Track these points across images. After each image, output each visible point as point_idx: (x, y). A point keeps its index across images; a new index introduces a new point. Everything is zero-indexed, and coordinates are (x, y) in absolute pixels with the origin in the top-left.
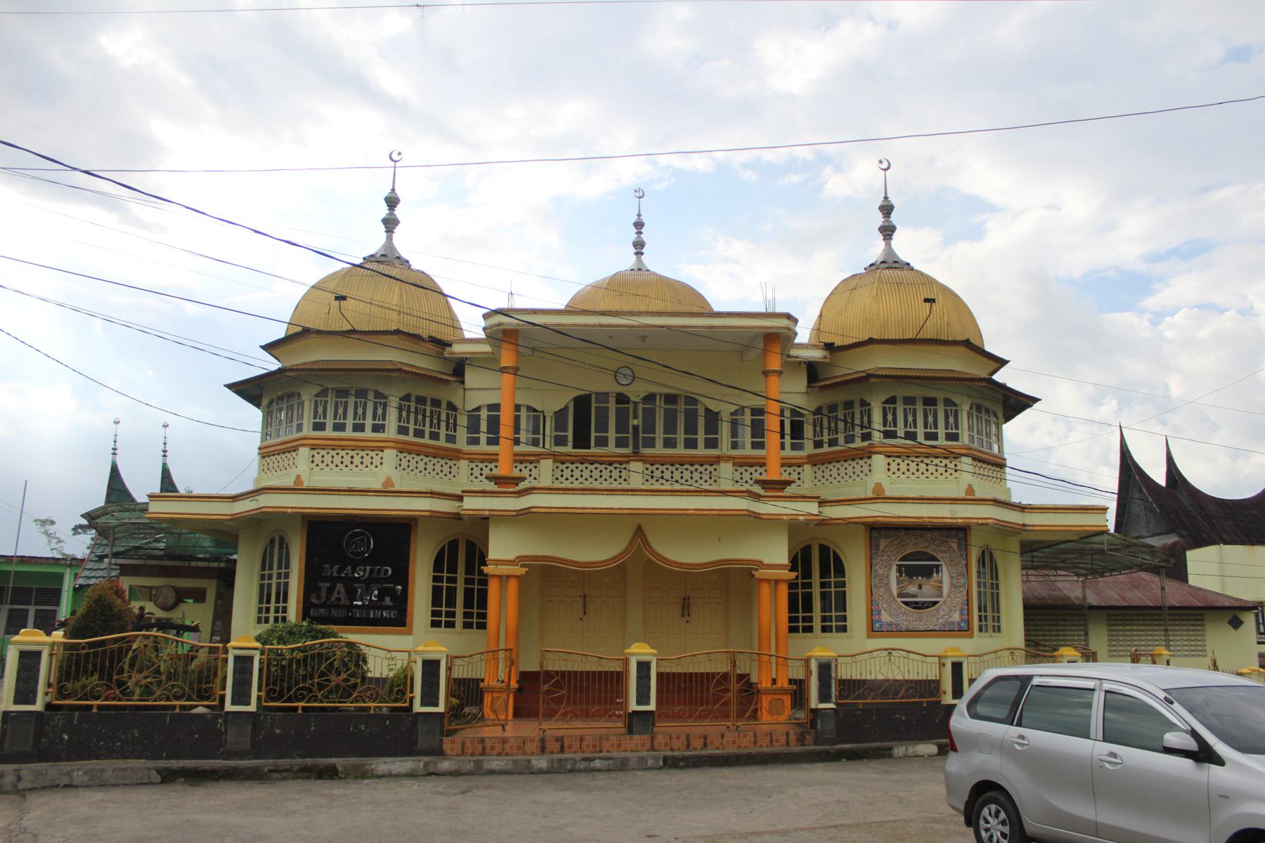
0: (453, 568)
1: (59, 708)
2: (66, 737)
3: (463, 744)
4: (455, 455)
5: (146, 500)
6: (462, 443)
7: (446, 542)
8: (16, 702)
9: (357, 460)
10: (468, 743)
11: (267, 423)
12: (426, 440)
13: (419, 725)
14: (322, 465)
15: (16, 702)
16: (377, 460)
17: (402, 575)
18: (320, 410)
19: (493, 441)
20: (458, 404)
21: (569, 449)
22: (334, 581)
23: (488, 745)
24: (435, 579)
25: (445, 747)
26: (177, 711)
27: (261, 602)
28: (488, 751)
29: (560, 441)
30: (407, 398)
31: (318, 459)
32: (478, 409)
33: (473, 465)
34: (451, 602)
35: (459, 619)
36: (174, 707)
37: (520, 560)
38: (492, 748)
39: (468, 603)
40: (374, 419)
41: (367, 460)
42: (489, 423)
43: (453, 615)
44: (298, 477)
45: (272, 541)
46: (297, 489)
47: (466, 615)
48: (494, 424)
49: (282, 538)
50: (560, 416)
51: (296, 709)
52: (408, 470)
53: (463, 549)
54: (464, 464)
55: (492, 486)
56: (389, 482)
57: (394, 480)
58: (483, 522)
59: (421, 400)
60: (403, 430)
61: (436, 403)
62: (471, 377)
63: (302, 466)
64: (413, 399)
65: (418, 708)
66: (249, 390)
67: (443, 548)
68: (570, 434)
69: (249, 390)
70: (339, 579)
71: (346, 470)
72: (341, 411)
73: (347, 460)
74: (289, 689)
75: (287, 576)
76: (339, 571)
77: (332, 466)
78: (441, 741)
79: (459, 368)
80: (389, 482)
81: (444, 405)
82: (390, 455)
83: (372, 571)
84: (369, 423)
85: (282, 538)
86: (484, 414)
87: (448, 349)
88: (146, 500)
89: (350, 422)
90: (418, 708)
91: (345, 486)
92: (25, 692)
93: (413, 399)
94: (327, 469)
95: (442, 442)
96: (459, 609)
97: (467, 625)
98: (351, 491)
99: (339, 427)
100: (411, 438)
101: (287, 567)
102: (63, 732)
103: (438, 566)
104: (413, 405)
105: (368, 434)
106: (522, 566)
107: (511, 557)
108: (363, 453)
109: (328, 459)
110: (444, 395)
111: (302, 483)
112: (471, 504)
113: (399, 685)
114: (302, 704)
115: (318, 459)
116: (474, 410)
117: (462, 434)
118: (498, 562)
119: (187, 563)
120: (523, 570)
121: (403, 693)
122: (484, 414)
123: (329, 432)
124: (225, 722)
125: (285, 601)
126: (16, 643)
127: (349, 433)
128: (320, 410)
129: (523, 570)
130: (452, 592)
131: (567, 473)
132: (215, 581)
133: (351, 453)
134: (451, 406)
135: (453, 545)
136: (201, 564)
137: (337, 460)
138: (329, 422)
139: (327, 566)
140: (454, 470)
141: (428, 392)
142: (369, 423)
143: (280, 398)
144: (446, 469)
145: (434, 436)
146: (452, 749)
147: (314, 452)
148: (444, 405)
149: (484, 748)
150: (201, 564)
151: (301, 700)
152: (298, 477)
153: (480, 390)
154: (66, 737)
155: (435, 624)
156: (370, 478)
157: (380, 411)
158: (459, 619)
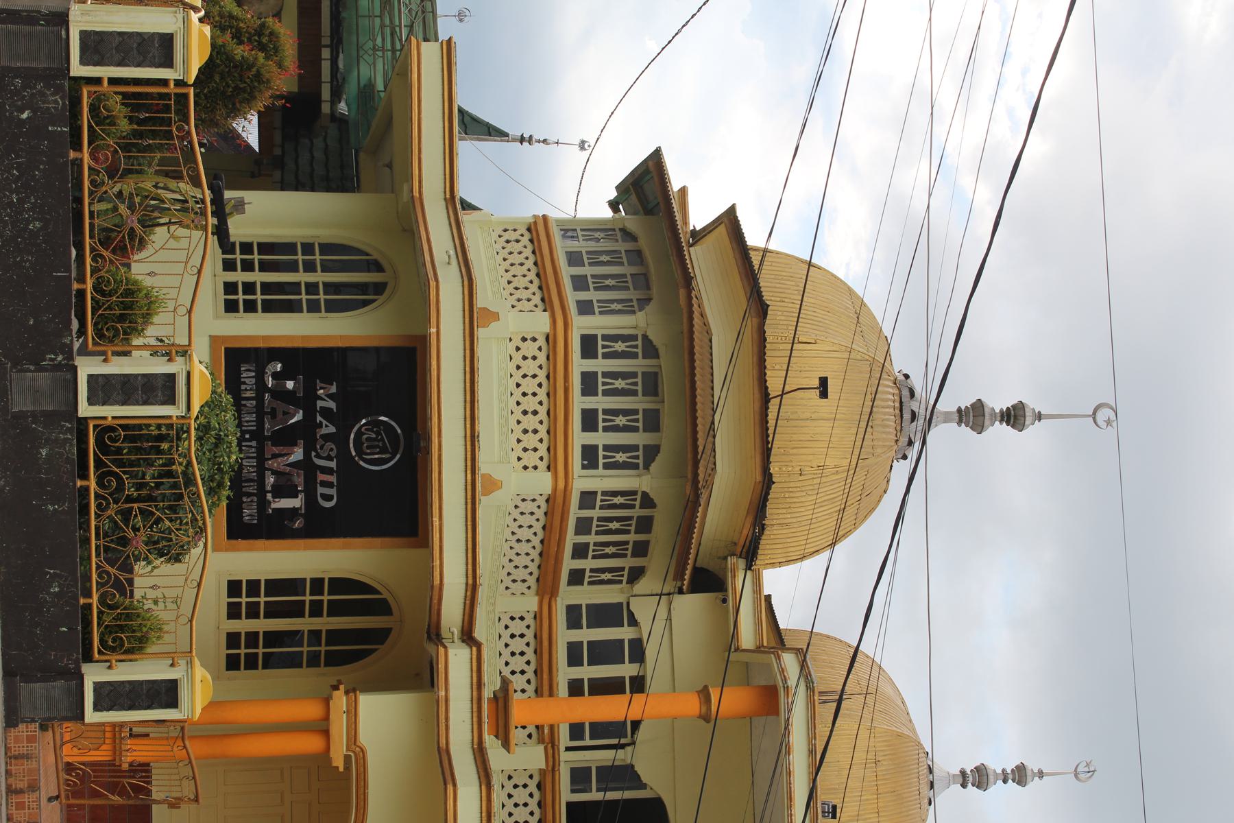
0: (336, 609)
1: (75, 102)
2: (25, 116)
3: (27, 757)
4: (546, 587)
5: (443, 36)
6: (569, 595)
7: (385, 595)
8: (84, 35)
9: (530, 422)
10: (27, 765)
11: (593, 229)
12: (571, 539)
13: (60, 683)
14: (518, 358)
15: (84, 35)
16: (531, 459)
17: (318, 525)
18: (620, 346)
19: (575, 688)
20: (642, 586)
21: (566, 795)
22: (307, 401)
23: (25, 798)
24: (317, 584)
25: (22, 727)
26: (75, 286)
27: (265, 248)
28: (15, 799)
29: (580, 777)
30: (647, 502)
31: (530, 349)
32: (633, 622)
33: (529, 620)
34: (273, 611)
35: (243, 625)
36: (81, 279)
37: (357, 757)
38: (20, 806)
39: (273, 638)
40: (607, 448)
41: (531, 441)
42: (613, 658)
43: (253, 613)
44: (495, 316)
45: (377, 266)
46: (473, 318)
47: (252, 638)
48: (603, 653)
49: (379, 288)
50: (625, 775)
51: (85, 476)
52: (516, 514)
53: (372, 638)
54: (530, 603)
55: (491, 685)
56: (493, 485)
57: (497, 495)
58: (422, 677)
59: (645, 525)
60: (588, 498)
61: (641, 549)
62: (690, 606)
63: (517, 322)
64: (646, 512)
65: (93, 675)
66: (648, 188)
67: (378, 592)
68: (594, 796)
69: (648, 188)
70: (310, 412)
71: (512, 403)
72: (619, 384)
73: (530, 404)
74: (120, 463)
75: (314, 307)
76: (326, 412)
77: (517, 377)
78: (33, 721)
79: (708, 581)
80: (493, 485)
81: (637, 562)
82: (542, 483)
83: (329, 471)
84: (599, 439)
85: (379, 288)
86: (624, 633)
87: (742, 563)
88: (443, 36)
89: (600, 402)
90: (93, 675)
91: (481, 427)
92: (99, 46)
93: (646, 512)
94: (511, 367)
95: (569, 564)
96: (262, 625)
97: (233, 639)
98: (472, 439)
99: (590, 421)
100: (574, 512)
101: (332, 307)
102: (34, 111)
103: (339, 584)
104: (637, 512)
105: (580, 438)
106: (347, 759)
107: (364, 738)
108: (542, 433)
109: (530, 367)
110: (658, 561)
111: (487, 492)
112: (457, 660)
113: (129, 633)
114: (93, 484)
115: (530, 349)
116: (631, 615)
117: (586, 595)
118: (353, 713)
119: (326, 41)
120: (339, 763)
121: (113, 649)
122: (624, 633)
123: (579, 365)
124: (57, 367)
125: (269, 307)
126: (186, 21)
127: (579, 402)
128: (620, 346)
129: (339, 763)
130: (295, 611)
131: (521, 796)
132: (296, 89)
133: (543, 411)
134: (636, 574)
135: (382, 607)
136: (326, 67)
137: (529, 385)
138: (598, 365)
139: (333, 389)
140: (520, 587)
141: (661, 536)
142: (599, 439)
143: (637, 256)
144: (521, 574)
145: (580, 551)
146: (17, 740)
147: (541, 341)
148: (637, 562)
149: (20, 792)
150: (326, 67)
151: (100, 483)
152: (495, 316)
153: (673, 627)
154: (25, 116)
155: (234, 587)
156: (500, 451)
157: (621, 457)
158: (243, 625)
